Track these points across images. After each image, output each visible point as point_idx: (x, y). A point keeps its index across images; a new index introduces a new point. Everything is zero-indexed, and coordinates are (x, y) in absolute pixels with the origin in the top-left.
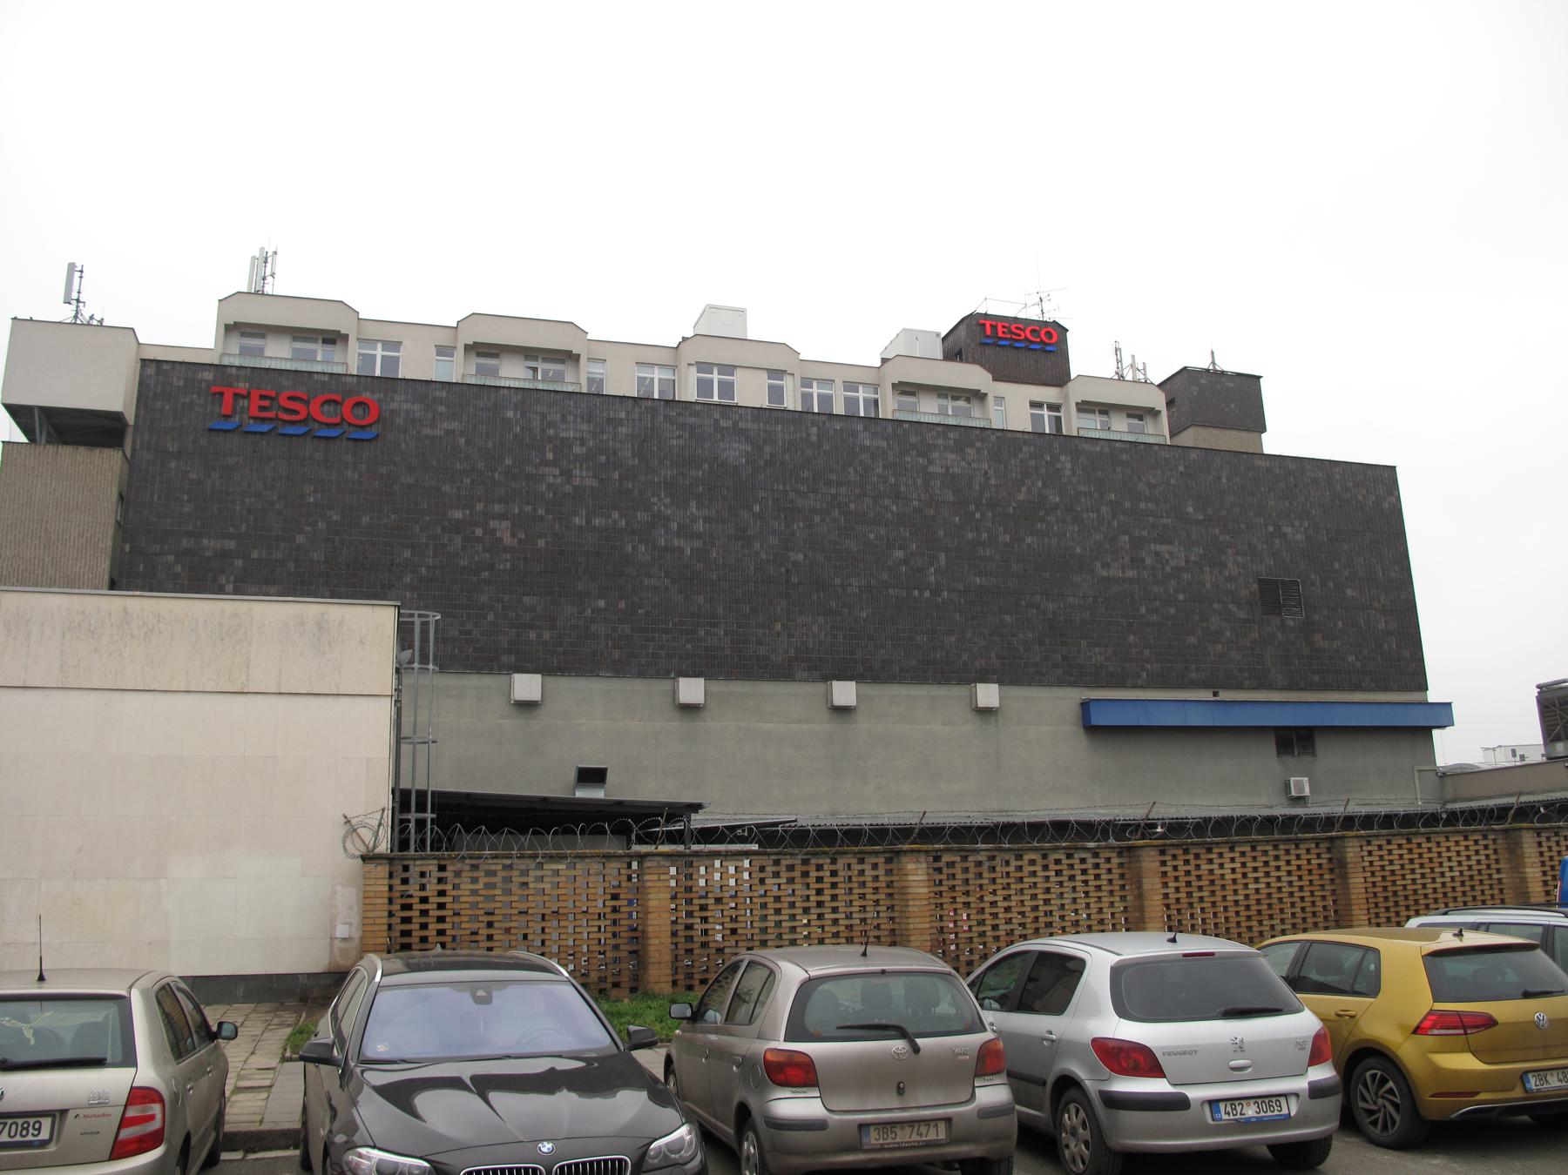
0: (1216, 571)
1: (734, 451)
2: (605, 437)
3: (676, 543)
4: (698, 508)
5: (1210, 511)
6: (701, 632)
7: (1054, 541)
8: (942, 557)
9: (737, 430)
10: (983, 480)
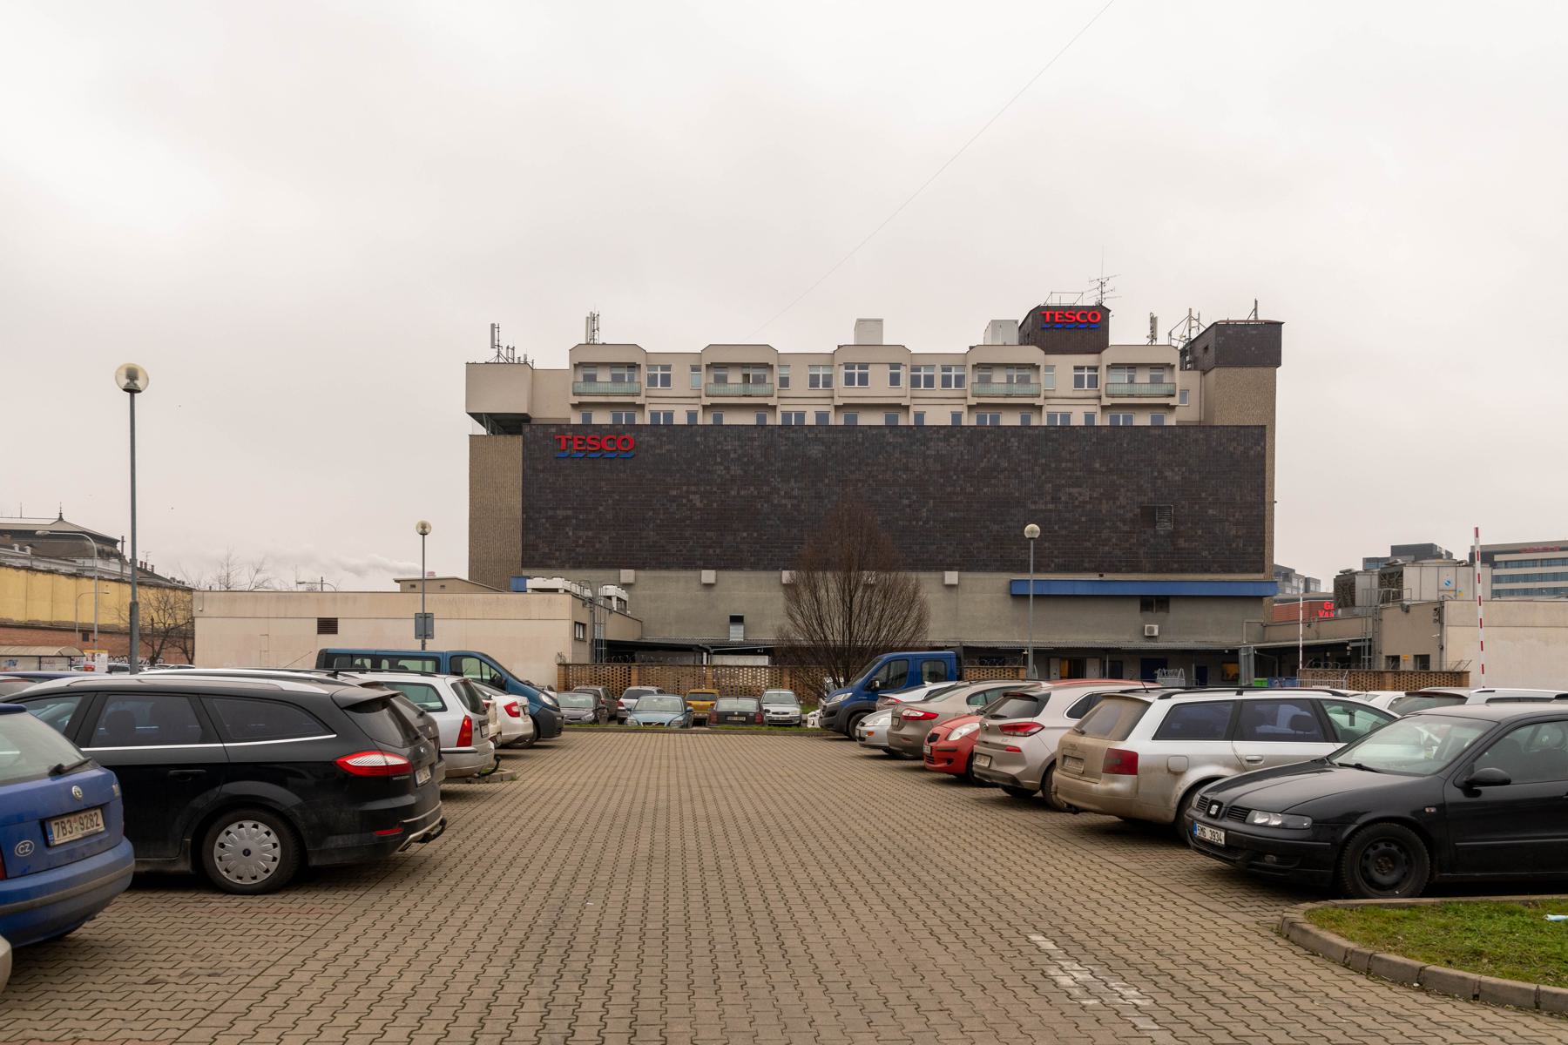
0: (1111, 502)
1: (815, 451)
2: (747, 448)
3: (784, 502)
4: (795, 482)
5: (1111, 466)
6: (796, 547)
7: (1002, 490)
8: (932, 501)
9: (817, 439)
10: (960, 457)
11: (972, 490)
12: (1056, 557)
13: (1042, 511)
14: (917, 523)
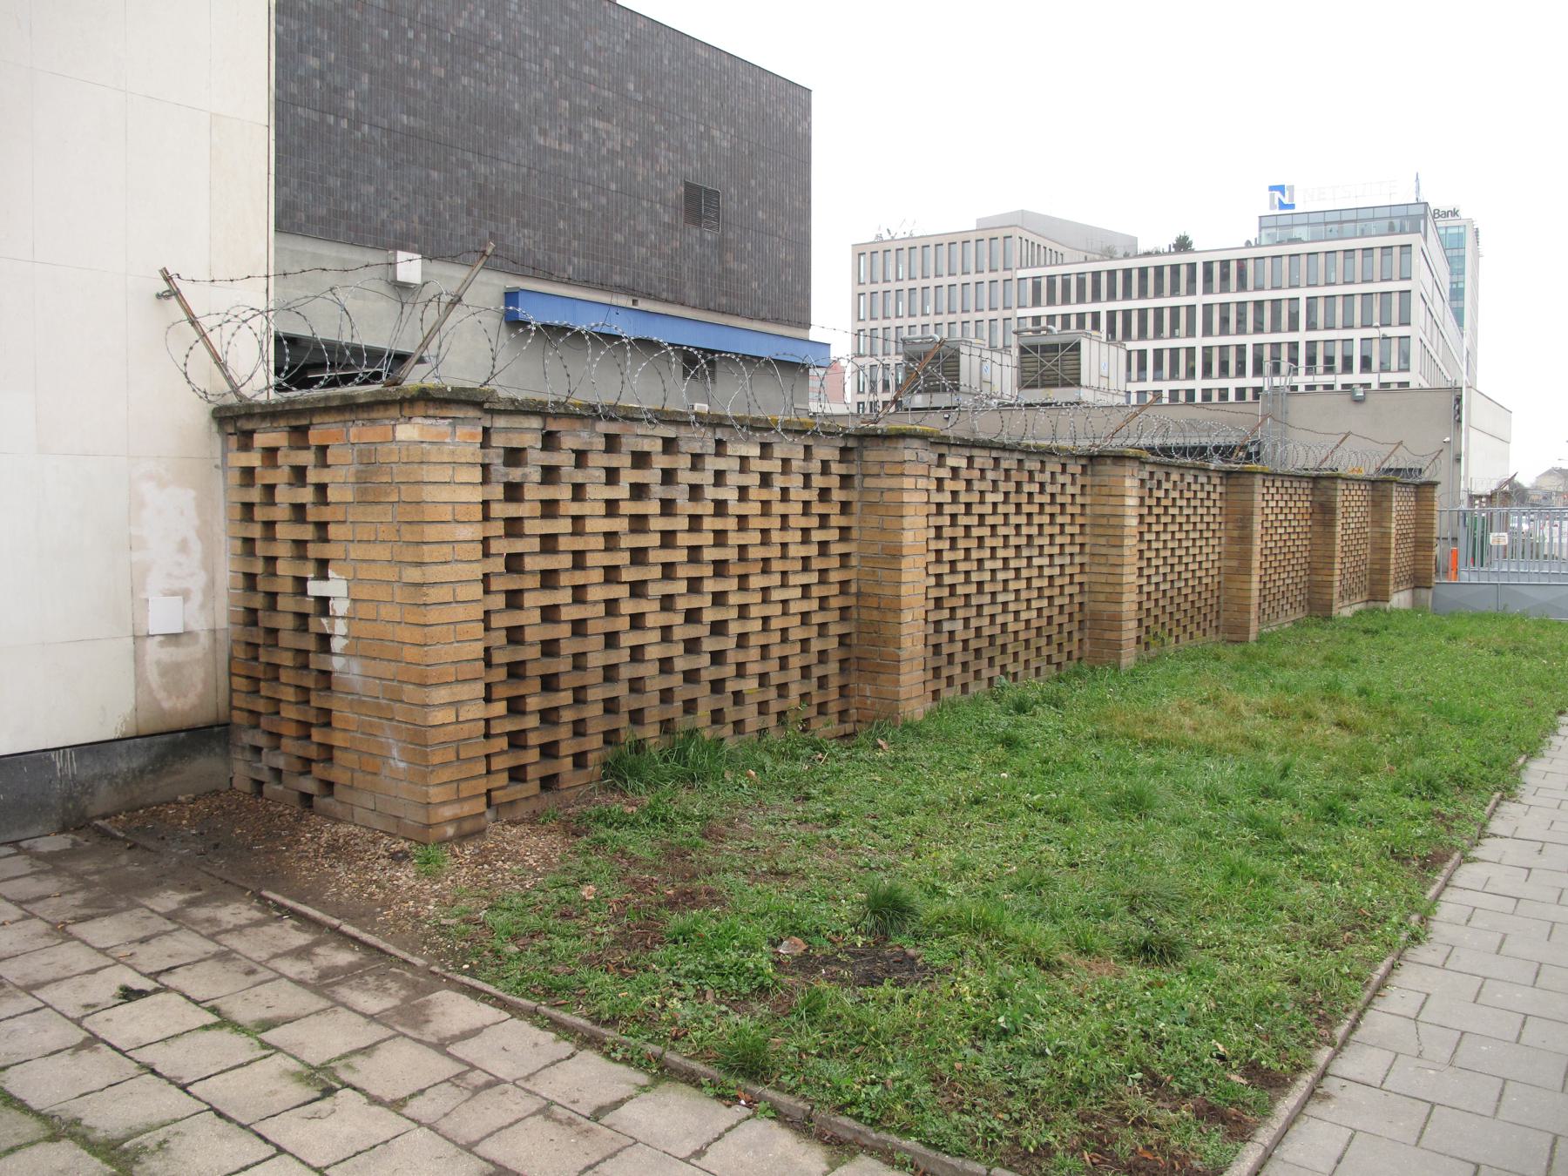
8: (365, 78)
11: (442, 73)
12: (576, 254)
13: (557, 154)
14: (337, 122)
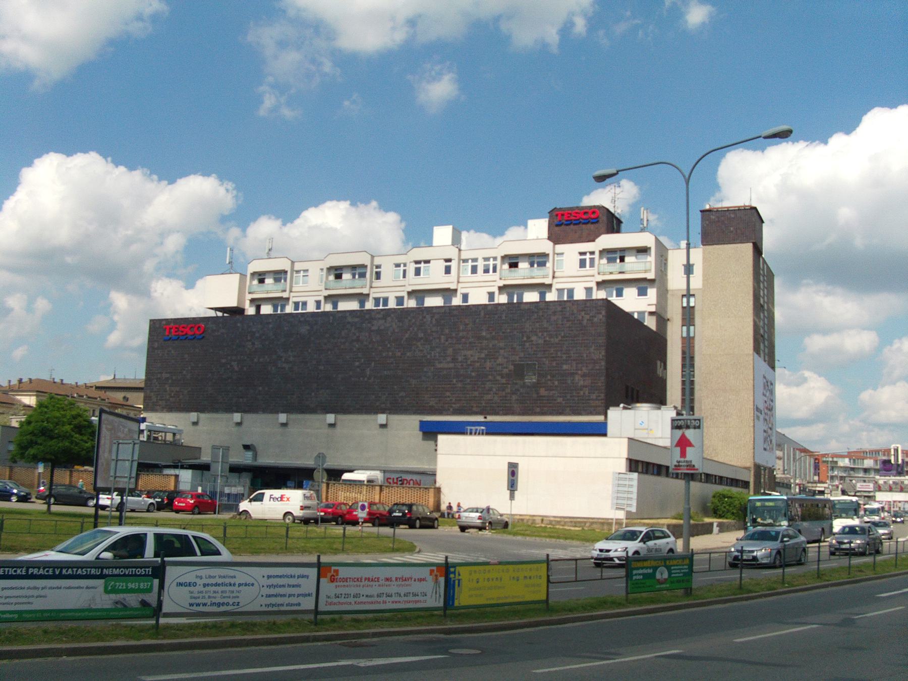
1: (304, 330)
